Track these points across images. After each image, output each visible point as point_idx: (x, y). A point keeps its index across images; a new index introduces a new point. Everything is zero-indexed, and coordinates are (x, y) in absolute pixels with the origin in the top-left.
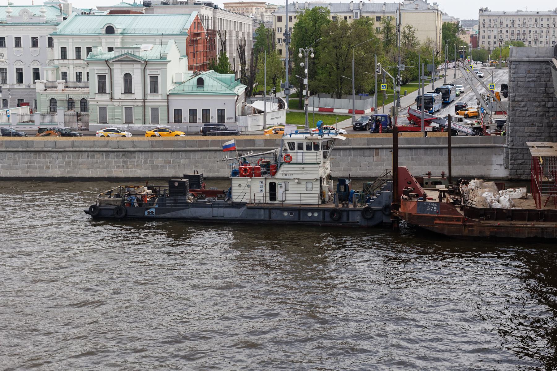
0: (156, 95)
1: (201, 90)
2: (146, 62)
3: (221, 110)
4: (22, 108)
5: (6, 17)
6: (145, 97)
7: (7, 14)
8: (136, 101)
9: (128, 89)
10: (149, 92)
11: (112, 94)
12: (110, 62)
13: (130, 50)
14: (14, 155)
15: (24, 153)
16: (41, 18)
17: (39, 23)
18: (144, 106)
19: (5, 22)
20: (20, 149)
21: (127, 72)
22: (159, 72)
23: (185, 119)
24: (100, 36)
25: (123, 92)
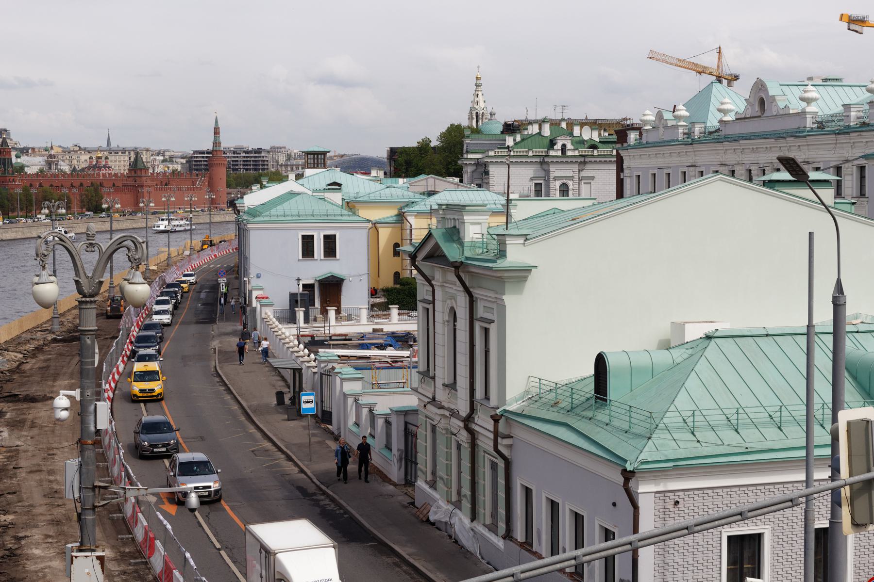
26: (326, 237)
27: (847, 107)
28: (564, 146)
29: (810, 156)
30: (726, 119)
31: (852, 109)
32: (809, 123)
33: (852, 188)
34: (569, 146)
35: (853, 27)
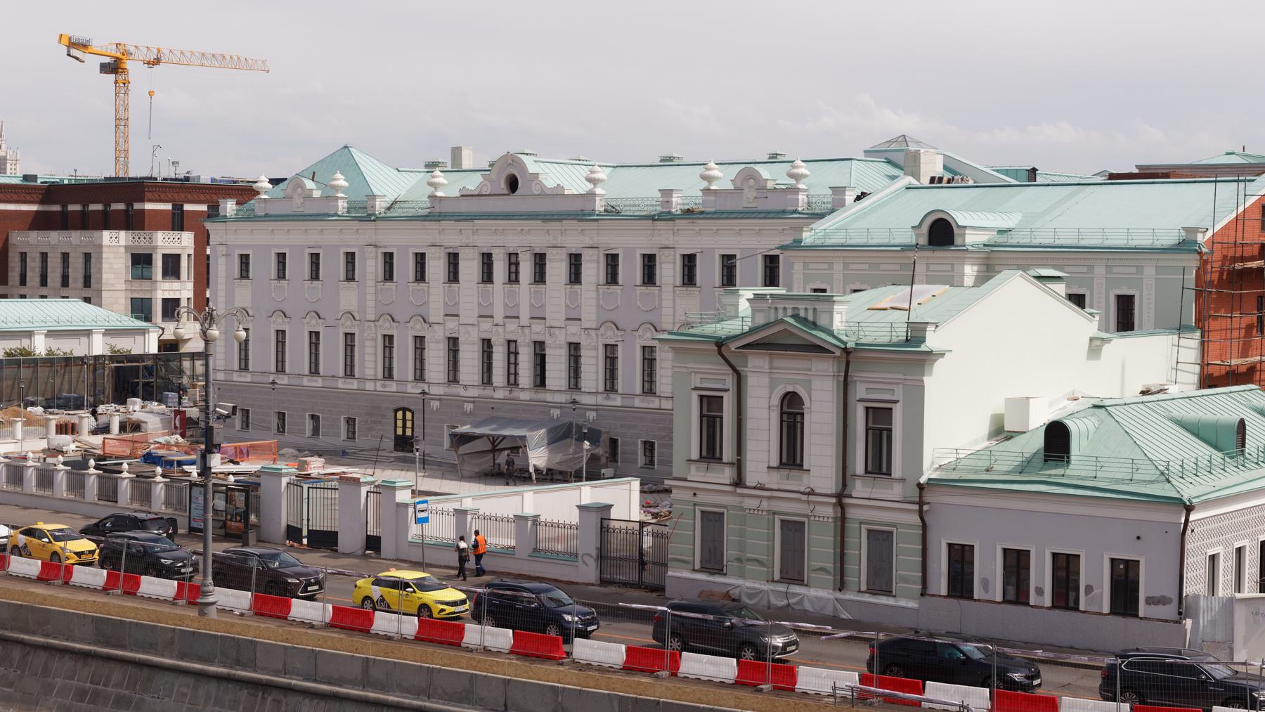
0: (882, 480)
1: (1055, 472)
2: (847, 351)
3: (1127, 562)
4: (536, 492)
5: (700, 194)
6: (844, 485)
7: (705, 184)
8: (812, 498)
9: (791, 457)
10: (860, 468)
11: (739, 466)
12: (733, 347)
13: (801, 306)
14: (195, 689)
15: (224, 685)
16: (790, 197)
17: (784, 212)
18: (843, 519)
19: (701, 208)
20: (213, 669)
21: (790, 389)
22: (898, 393)
23: (986, 585)
24: (910, 254)
25: (775, 462)
27: (667, 193)
29: (599, 242)
30: (439, 194)
31: (674, 195)
32: (599, 206)
33: (674, 276)
35: (74, 52)
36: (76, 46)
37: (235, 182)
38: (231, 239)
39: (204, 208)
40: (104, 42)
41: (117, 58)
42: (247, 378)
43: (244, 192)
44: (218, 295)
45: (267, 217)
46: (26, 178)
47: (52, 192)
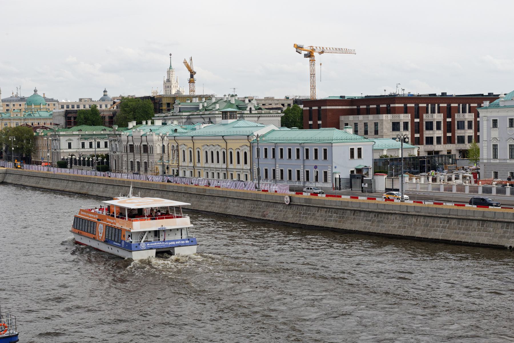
26: (358, 149)
28: (250, 108)
34: (253, 109)
36: (299, 48)
37: (420, 96)
38: (489, 114)
39: (476, 105)
40: (307, 46)
41: (311, 52)
42: (497, 161)
43: (492, 98)
44: (483, 134)
45: (505, 107)
46: (341, 97)
47: (352, 101)
